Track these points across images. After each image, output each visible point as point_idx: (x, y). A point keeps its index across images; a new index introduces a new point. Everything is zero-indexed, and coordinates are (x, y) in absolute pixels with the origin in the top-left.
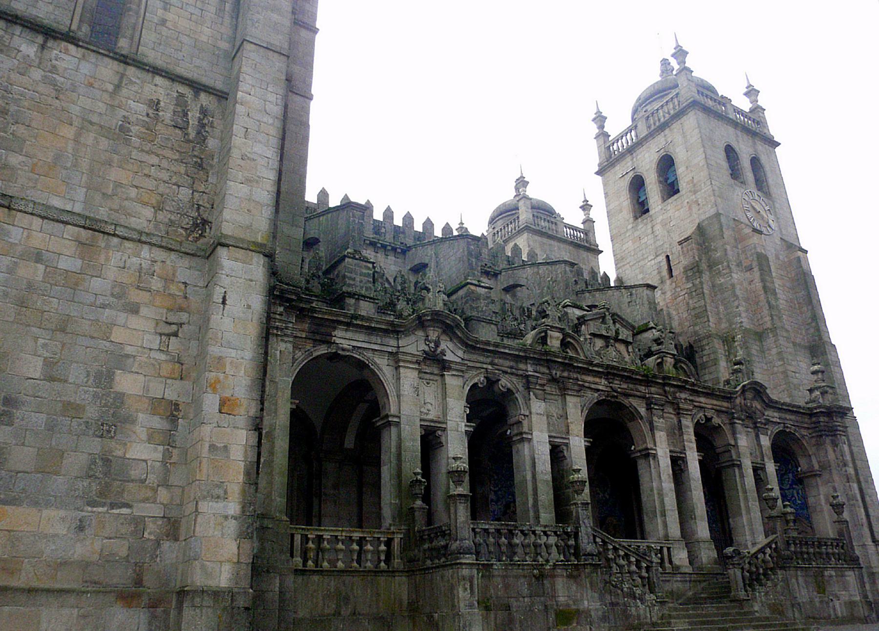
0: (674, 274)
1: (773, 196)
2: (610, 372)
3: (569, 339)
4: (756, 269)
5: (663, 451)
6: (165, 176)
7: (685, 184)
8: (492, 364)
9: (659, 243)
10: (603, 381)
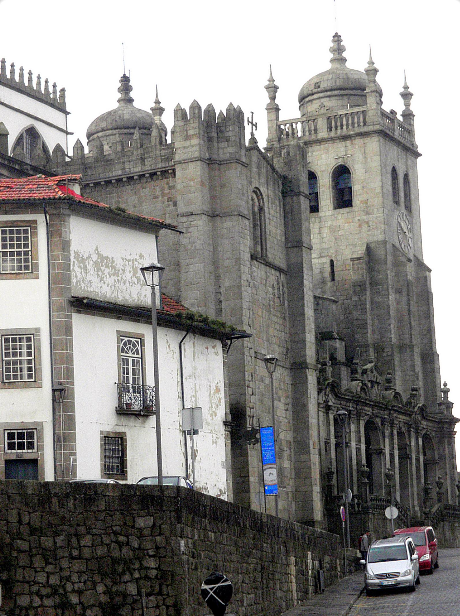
0: (337, 278)
1: (413, 211)
2: (376, 405)
3: (365, 387)
4: (404, 293)
5: (387, 451)
6: (278, 327)
7: (358, 202)
8: (340, 404)
9: (325, 246)
10: (370, 409)
